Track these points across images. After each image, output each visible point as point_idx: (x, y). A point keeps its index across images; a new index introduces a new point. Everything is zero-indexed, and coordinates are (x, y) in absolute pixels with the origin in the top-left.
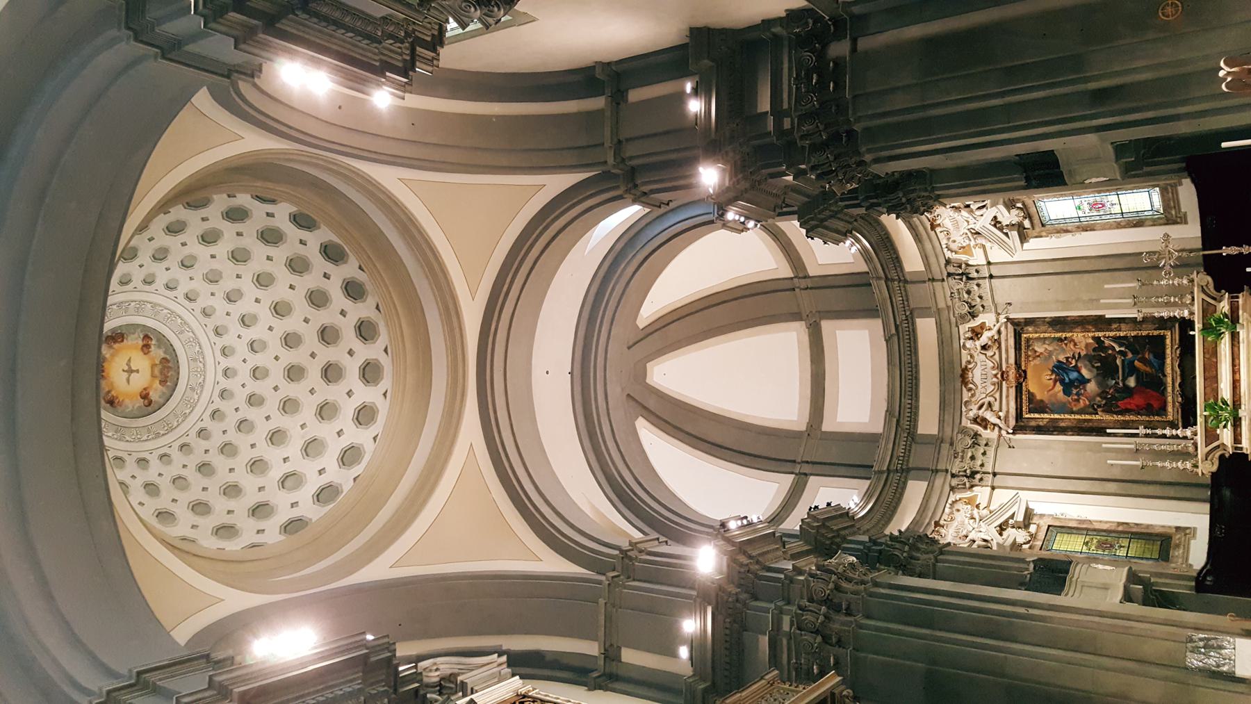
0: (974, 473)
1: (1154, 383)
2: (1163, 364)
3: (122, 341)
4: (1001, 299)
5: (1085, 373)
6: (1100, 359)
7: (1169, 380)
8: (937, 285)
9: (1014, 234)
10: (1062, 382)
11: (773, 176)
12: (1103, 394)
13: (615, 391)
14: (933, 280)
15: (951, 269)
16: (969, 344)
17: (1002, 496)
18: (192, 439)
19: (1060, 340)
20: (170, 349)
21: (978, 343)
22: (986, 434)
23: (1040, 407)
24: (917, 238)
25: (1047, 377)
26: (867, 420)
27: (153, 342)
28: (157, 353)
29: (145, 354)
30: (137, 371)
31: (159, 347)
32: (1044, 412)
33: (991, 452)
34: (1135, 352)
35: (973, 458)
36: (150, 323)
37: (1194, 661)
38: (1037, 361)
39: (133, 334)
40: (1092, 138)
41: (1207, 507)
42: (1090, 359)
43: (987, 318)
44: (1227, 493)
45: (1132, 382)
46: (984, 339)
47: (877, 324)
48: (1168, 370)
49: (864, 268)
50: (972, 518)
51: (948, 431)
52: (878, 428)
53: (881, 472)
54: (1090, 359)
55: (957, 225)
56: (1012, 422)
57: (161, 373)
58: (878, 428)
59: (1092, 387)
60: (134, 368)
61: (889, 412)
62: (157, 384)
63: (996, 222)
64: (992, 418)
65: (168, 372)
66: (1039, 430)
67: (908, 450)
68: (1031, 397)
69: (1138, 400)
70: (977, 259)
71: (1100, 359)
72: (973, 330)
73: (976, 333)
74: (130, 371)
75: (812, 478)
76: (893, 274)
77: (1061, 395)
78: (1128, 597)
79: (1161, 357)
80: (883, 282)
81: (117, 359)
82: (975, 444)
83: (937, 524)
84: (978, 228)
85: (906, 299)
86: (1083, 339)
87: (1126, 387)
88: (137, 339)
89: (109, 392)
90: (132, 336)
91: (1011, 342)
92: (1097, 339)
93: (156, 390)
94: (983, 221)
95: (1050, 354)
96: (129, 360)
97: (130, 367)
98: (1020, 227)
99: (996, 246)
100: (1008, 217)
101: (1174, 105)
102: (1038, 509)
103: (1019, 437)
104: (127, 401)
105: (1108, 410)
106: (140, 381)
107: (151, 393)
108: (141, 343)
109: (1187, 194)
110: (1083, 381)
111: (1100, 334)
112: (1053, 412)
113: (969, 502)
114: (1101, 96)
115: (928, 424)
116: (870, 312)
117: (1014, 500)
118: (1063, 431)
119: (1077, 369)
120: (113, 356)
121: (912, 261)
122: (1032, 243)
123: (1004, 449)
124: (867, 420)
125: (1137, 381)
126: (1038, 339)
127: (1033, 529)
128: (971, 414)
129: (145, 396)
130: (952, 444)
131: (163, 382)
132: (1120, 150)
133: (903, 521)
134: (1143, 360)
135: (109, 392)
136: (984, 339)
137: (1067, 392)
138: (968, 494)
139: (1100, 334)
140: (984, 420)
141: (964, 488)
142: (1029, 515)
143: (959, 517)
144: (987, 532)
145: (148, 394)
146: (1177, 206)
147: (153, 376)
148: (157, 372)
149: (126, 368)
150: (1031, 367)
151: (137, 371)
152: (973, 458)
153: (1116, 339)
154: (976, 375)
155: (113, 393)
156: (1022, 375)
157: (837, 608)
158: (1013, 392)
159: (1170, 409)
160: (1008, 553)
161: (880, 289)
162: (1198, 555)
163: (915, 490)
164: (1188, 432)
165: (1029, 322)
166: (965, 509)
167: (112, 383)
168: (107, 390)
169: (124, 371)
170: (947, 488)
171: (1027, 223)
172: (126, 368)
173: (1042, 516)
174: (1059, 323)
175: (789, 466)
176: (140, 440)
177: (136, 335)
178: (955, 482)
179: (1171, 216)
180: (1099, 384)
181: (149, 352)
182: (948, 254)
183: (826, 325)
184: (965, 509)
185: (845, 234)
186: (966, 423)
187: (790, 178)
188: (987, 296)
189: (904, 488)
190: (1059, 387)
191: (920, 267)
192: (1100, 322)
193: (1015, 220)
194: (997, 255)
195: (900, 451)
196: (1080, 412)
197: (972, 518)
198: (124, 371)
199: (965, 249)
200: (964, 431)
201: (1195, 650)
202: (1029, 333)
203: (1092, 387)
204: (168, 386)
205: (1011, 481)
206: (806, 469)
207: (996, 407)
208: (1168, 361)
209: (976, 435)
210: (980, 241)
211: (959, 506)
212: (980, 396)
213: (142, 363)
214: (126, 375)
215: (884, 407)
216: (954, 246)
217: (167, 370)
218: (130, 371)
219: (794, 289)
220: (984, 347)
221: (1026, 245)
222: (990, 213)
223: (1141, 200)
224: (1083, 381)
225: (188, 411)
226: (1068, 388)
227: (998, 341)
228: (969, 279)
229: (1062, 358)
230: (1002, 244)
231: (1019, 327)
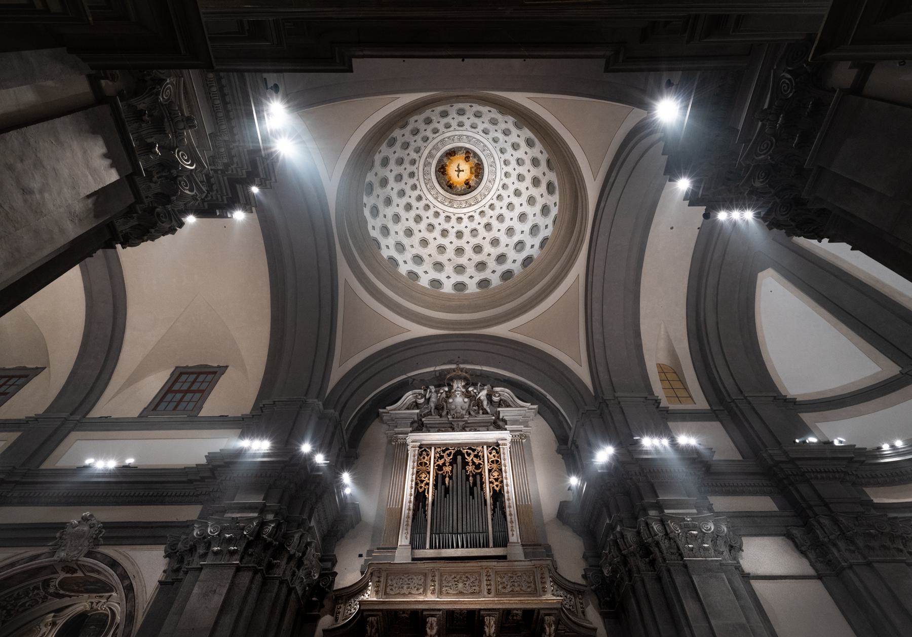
3: (455, 155)
18: (486, 209)
20: (480, 159)
27: (471, 155)
28: (474, 161)
29: (467, 162)
30: (463, 171)
31: (475, 157)
36: (468, 146)
39: (460, 151)
57: (476, 172)
60: (461, 169)
62: (473, 177)
65: (480, 171)
74: (459, 171)
81: (452, 165)
88: (462, 154)
89: (448, 182)
90: (460, 152)
93: (473, 180)
96: (459, 165)
97: (459, 169)
104: (458, 186)
106: (464, 176)
107: (470, 182)
108: (464, 156)
120: (450, 163)
129: (467, 183)
131: (476, 176)
135: (448, 182)
145: (469, 182)
147: (471, 173)
148: (473, 170)
149: (457, 169)
151: (463, 171)
155: (451, 182)
167: (450, 177)
168: (448, 180)
169: (456, 171)
172: (457, 169)
176: (461, 207)
177: (462, 152)
181: (469, 160)
198: (456, 171)
204: (479, 178)
213: (465, 167)
214: (457, 173)
217: (478, 170)
218: (459, 171)
225: (486, 193)
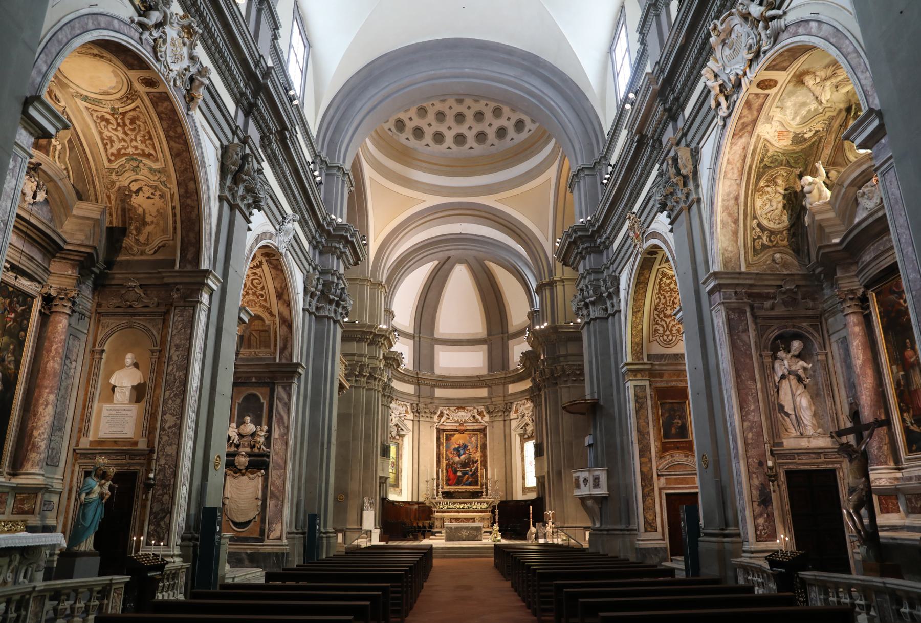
0: (419, 413)
1: (459, 482)
2: (466, 485)
4: (495, 424)
5: (463, 457)
6: (468, 463)
7: (460, 487)
8: (502, 398)
9: (522, 431)
10: (459, 448)
11: (544, 350)
12: (454, 463)
13: (452, 253)
14: (504, 396)
15: (509, 404)
16: (476, 411)
17: (409, 424)
19: (477, 447)
21: (476, 414)
22: (436, 418)
23: (448, 438)
24: (522, 392)
25: (461, 442)
26: (440, 365)
32: (446, 440)
33: (428, 419)
34: (472, 475)
35: (425, 412)
37: (366, 499)
38: (468, 438)
40: (546, 470)
41: (410, 500)
42: (469, 458)
43: (487, 418)
44: (416, 506)
45: (459, 474)
46: (478, 417)
47: (485, 372)
48: (464, 487)
49: (511, 368)
50: (400, 413)
51: (436, 401)
52: (437, 372)
53: (417, 375)
54: (469, 458)
55: (527, 409)
56: (441, 428)
58: (437, 372)
59: (457, 459)
61: (444, 377)
63: (527, 425)
64: (442, 420)
66: (438, 439)
67: (427, 385)
68: (453, 435)
69: (452, 476)
70: (513, 415)
71: (468, 463)
72: (482, 412)
73: (480, 413)
75: (412, 342)
76: (507, 380)
77: (454, 447)
78: (381, 477)
79: (470, 484)
80: (503, 376)
82: (431, 413)
83: (397, 400)
84: (525, 417)
85: (497, 385)
86: (477, 456)
87: (457, 472)
91: (476, 428)
92: (477, 461)
94: (527, 419)
95: (471, 443)
98: (525, 434)
99: (517, 424)
100: (530, 429)
101: (554, 496)
102: (405, 439)
103: (435, 430)
105: (447, 465)
109: (532, 496)
110: (459, 456)
111: (479, 462)
112: (446, 444)
113: (407, 412)
114: (559, 473)
115: (439, 393)
116: (491, 367)
117: (408, 429)
118: (438, 447)
119: (464, 453)
121: (512, 388)
122: (518, 438)
123: (430, 425)
124: (440, 365)
125: (460, 476)
126: (477, 438)
127: (397, 437)
128: (444, 411)
130: (431, 403)
132: (544, 477)
133: (396, 385)
134: (468, 478)
136: (478, 417)
137: (455, 449)
138: (409, 411)
139: (479, 462)
140: (442, 416)
141: (412, 409)
142: (402, 436)
143: (400, 408)
144: (394, 419)
146: (529, 492)
150: (465, 435)
152: (425, 412)
153: (477, 468)
154: (462, 413)
156: (462, 432)
157: (369, 378)
158: (455, 428)
159: (449, 487)
160: (389, 429)
161: (501, 374)
162: (393, 497)
163: (410, 389)
164: (440, 496)
165: (485, 435)
166: (402, 410)
170: (412, 402)
171: (526, 436)
173: (403, 440)
174: (484, 447)
175: (417, 331)
178: (414, 405)
179: (525, 490)
180: (458, 462)
182: (515, 403)
183: (485, 347)
184: (402, 410)
185: (524, 366)
186: (440, 409)
187: (542, 358)
188: (498, 418)
189: (411, 384)
190: (457, 446)
191: (510, 392)
192: (484, 465)
193: (528, 432)
194: (514, 424)
195: (427, 382)
196: (446, 455)
197: (400, 413)
199: (516, 411)
200: (437, 408)
201: (369, 500)
202: (480, 435)
203: (457, 459)
205: (416, 428)
206: (417, 339)
207: (448, 421)
208: (468, 487)
209: (435, 413)
210: (520, 418)
211: (404, 408)
212: (452, 415)
215: (447, 374)
216: (518, 406)
219: (502, 333)
220: (474, 417)
221: (517, 436)
222: (530, 423)
223: (531, 482)
224: (459, 456)
226: (457, 450)
227: (477, 422)
228: (504, 412)
229: (469, 447)
230: (518, 426)
231: (483, 431)
